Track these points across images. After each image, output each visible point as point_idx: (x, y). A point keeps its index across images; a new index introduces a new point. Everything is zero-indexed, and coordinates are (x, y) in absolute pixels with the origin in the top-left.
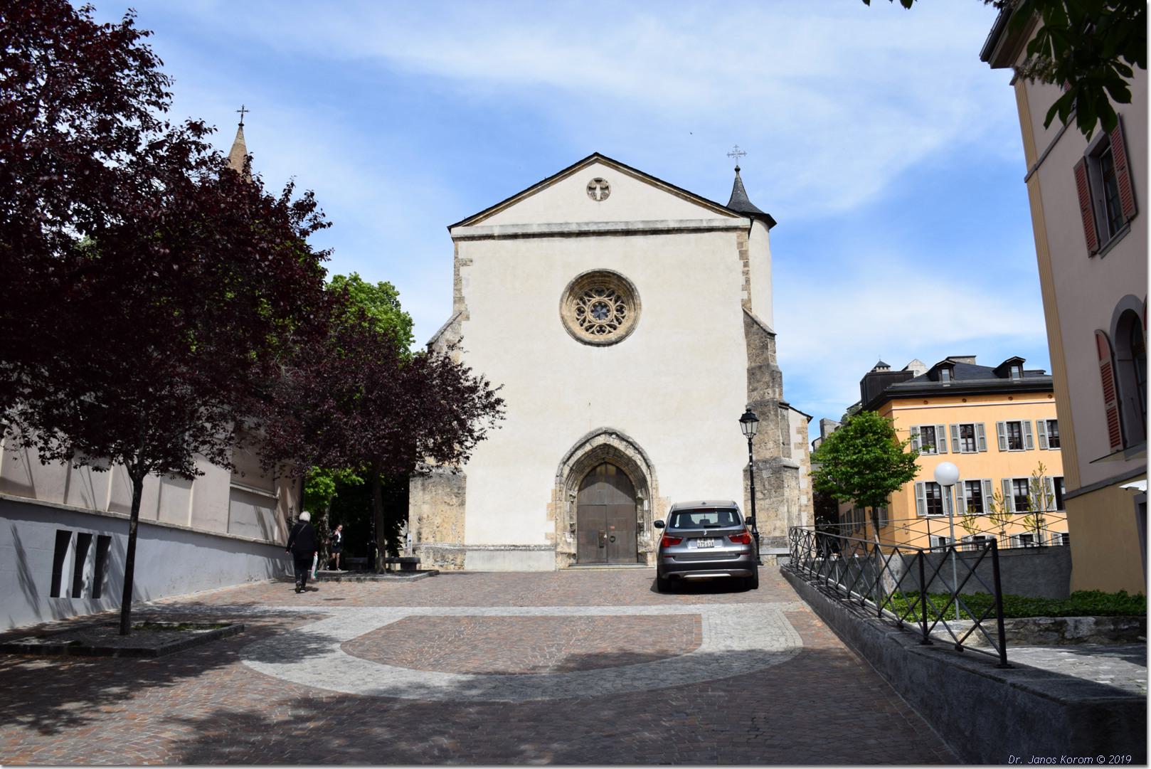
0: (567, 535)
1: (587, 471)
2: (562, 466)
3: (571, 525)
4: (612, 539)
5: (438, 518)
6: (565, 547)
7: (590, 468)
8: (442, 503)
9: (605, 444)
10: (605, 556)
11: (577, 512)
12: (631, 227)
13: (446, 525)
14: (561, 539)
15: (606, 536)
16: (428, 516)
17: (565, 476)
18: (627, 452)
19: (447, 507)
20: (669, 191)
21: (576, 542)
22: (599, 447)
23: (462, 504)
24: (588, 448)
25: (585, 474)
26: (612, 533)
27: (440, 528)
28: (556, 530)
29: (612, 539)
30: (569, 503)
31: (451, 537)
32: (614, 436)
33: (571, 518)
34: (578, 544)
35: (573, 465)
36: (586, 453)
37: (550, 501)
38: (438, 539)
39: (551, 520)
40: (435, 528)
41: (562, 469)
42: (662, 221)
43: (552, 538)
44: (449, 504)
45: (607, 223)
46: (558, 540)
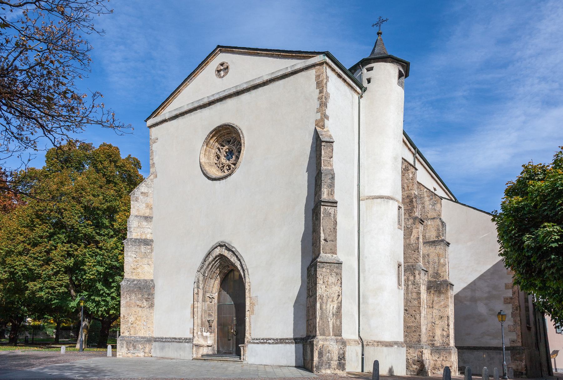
5: (132, 317)
8: (135, 306)
12: (239, 89)
13: (138, 322)
16: (124, 316)
19: (140, 309)
20: (267, 55)
23: (152, 306)
24: (211, 259)
27: (134, 325)
31: (143, 331)
38: (132, 332)
40: (129, 324)
42: (259, 78)
44: (141, 307)
45: (224, 91)
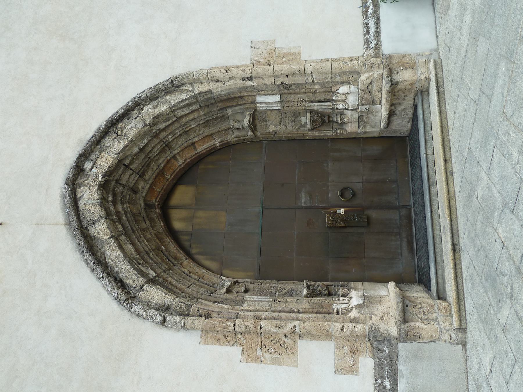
0: (339, 304)
1: (173, 248)
2: (137, 308)
3: (312, 294)
4: (349, 195)
6: (379, 310)
7: (168, 240)
9: (104, 186)
10: (394, 216)
11: (278, 279)
14: (355, 321)
15: (342, 211)
17: (167, 299)
18: (131, 134)
21: (359, 285)
22: (103, 202)
25: (181, 255)
26: (333, 195)
28: (328, 336)
29: (349, 195)
30: (248, 297)
32: (88, 165)
33: (290, 294)
34: (363, 280)
35: (143, 275)
36: (116, 238)
37: (237, 350)
39: (294, 351)
41: (148, 305)
43: (354, 351)
46: (360, 328)
